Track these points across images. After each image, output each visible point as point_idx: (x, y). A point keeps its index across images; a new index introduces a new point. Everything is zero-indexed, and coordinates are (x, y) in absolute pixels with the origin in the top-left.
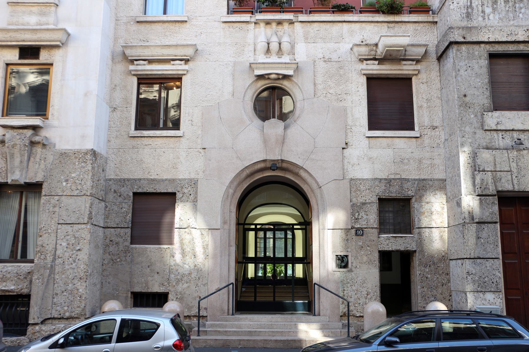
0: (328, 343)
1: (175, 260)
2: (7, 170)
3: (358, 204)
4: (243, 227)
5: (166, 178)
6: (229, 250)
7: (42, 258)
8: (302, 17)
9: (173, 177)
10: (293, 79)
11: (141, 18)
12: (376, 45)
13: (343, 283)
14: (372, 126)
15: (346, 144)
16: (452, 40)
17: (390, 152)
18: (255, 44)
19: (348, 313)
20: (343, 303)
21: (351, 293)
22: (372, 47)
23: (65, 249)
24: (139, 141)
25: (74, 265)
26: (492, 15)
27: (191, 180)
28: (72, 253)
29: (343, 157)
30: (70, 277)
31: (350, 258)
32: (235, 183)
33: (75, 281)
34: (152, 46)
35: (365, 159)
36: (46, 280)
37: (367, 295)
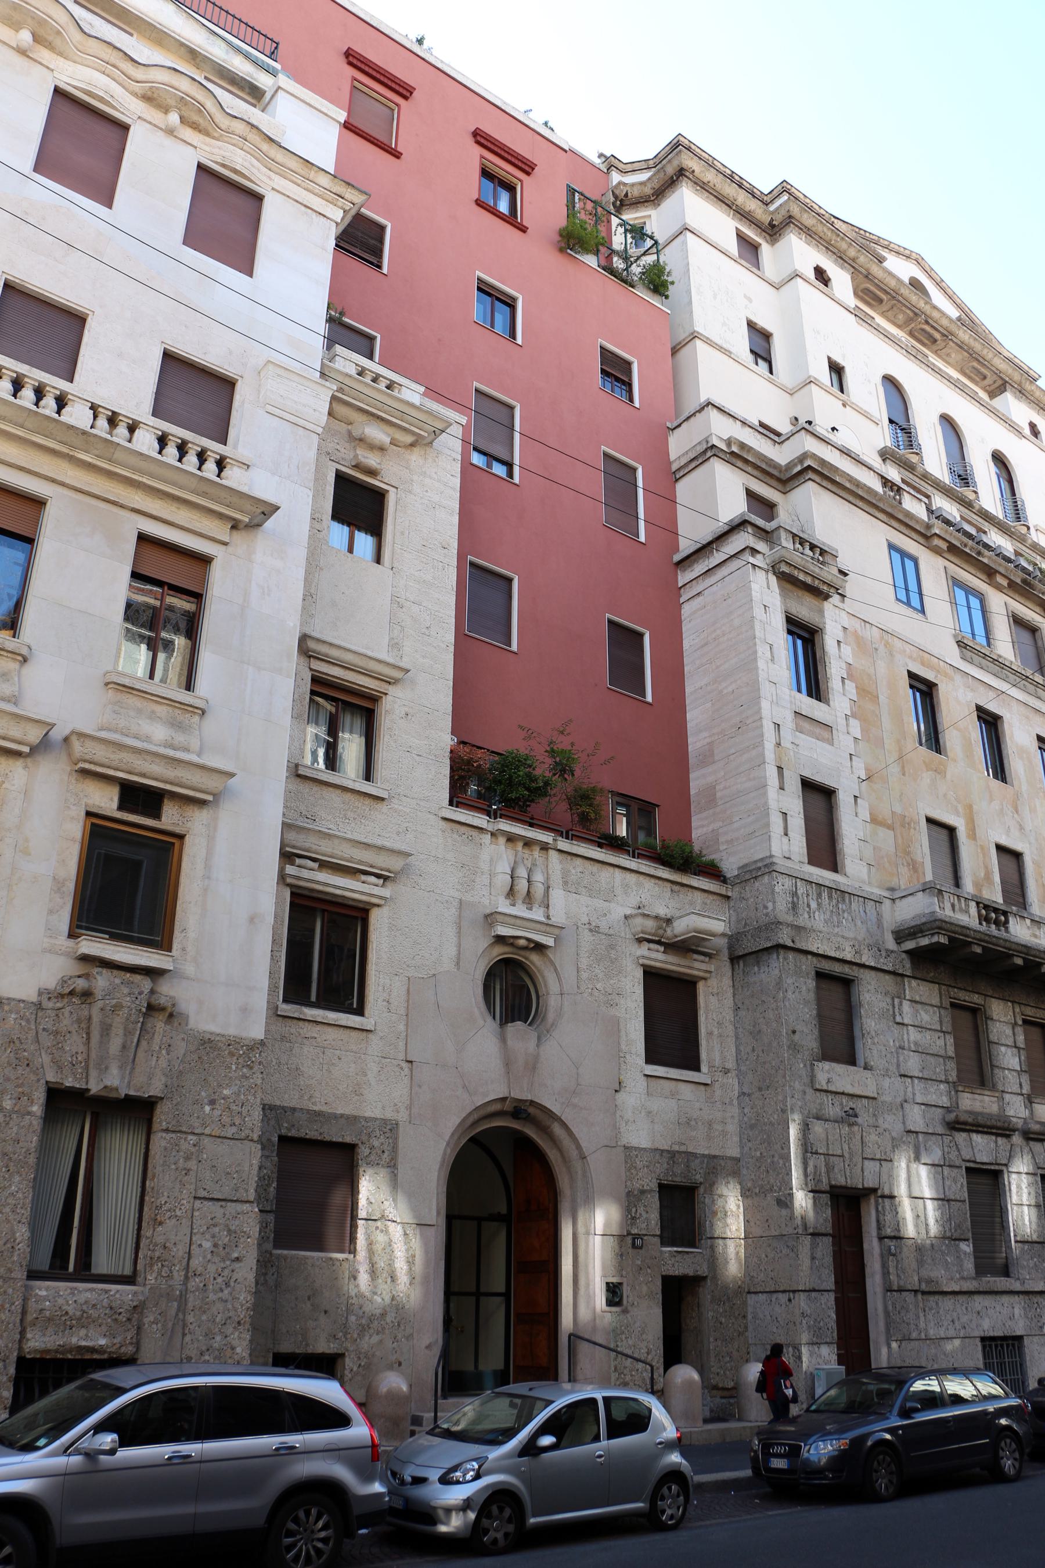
1: (357, 1286)
2: (87, 1061)
3: (636, 1193)
5: (342, 1112)
7: (164, 1274)
8: (563, 844)
9: (355, 1113)
11: (320, 774)
12: (669, 921)
13: (616, 1332)
14: (650, 1059)
16: (781, 941)
17: (672, 1103)
22: (661, 922)
23: (209, 1256)
24: (293, 1028)
25: (226, 1292)
26: (817, 913)
27: (385, 1121)
28: (222, 1265)
30: (218, 1320)
33: (229, 1329)
34: (338, 837)
36: (170, 1325)
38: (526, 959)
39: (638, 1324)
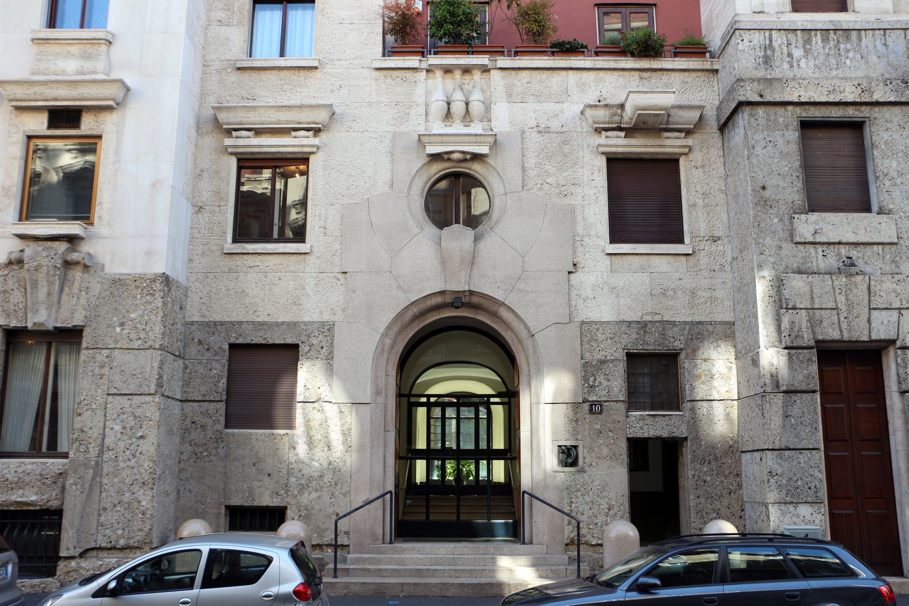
0: (546, 587)
1: (297, 455)
2: (26, 308)
3: (594, 363)
4: (407, 400)
5: (283, 320)
6: (385, 437)
8: (503, 62)
10: (490, 161)
12: (622, 106)
13: (569, 490)
14: (615, 238)
15: (575, 265)
16: (742, 99)
17: (645, 277)
18: (427, 105)
19: (578, 540)
20: (569, 523)
21: (582, 507)
22: (615, 109)
23: (119, 436)
24: (239, 261)
25: (133, 461)
27: (323, 324)
28: (130, 442)
29: (570, 286)
30: (126, 481)
31: (580, 450)
32: (395, 329)
33: (135, 488)
34: (261, 107)
35: (605, 289)
36: (87, 485)
37: (609, 510)
38: (470, 169)
39: (597, 483)
